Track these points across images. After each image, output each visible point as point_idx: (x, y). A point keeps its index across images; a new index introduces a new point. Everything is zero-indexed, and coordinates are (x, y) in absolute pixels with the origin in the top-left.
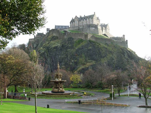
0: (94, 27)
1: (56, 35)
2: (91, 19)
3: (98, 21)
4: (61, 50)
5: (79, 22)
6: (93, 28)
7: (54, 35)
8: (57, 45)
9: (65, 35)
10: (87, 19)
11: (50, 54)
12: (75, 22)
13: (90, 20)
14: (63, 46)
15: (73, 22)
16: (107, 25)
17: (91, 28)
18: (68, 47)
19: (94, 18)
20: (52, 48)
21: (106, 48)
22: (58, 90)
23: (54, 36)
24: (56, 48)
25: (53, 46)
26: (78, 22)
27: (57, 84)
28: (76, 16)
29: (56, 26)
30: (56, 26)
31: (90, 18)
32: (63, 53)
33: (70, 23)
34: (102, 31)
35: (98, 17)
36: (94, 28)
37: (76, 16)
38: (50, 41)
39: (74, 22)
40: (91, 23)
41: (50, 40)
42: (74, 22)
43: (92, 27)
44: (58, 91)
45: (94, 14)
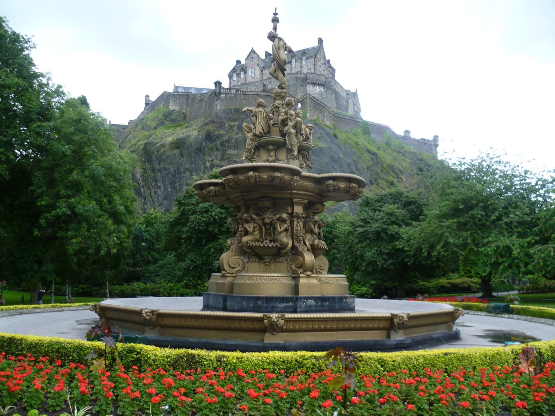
0: (319, 85)
1: (177, 108)
2: (307, 59)
3: (331, 70)
4: (199, 151)
5: (264, 72)
6: (319, 89)
7: (173, 106)
8: (185, 134)
9: (218, 98)
10: (294, 61)
11: (153, 170)
12: (249, 72)
13: (304, 63)
14: (209, 137)
15: (240, 74)
16: (355, 94)
17: (310, 89)
18: (228, 141)
19: (319, 56)
20: (163, 146)
21: (375, 154)
22: (296, 278)
23: (171, 113)
24: (179, 144)
25: (170, 139)
26: (258, 72)
27: (268, 217)
28: (253, 51)
29: (176, 88)
30: (176, 88)
31: (304, 58)
32: (208, 164)
33: (230, 76)
34: (347, 102)
35: (329, 61)
36: (321, 89)
37: (253, 51)
38: (155, 128)
39: (245, 73)
40: (305, 71)
41: (153, 125)
42: (245, 73)
43: (314, 84)
44: (296, 288)
45: (316, 44)
